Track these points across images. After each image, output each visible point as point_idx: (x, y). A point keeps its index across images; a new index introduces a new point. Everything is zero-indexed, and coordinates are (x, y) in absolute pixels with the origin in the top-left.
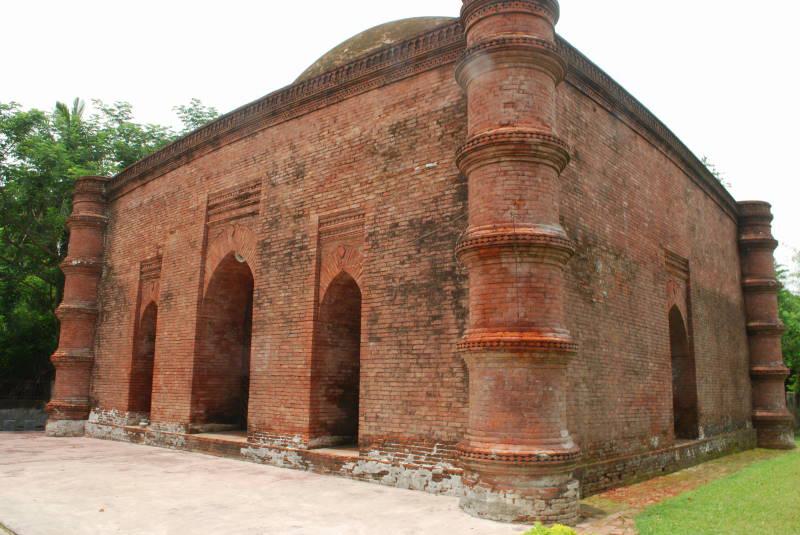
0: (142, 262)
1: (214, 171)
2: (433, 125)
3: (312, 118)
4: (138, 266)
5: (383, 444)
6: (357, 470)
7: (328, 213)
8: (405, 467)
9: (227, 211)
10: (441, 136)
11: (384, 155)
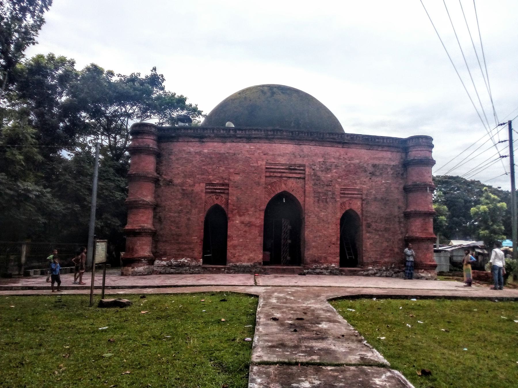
0: (206, 183)
1: (271, 153)
2: (389, 170)
3: (333, 149)
4: (203, 185)
5: (374, 263)
6: (365, 273)
7: (345, 187)
8: (384, 271)
9: (280, 172)
10: (392, 174)
11: (370, 173)
